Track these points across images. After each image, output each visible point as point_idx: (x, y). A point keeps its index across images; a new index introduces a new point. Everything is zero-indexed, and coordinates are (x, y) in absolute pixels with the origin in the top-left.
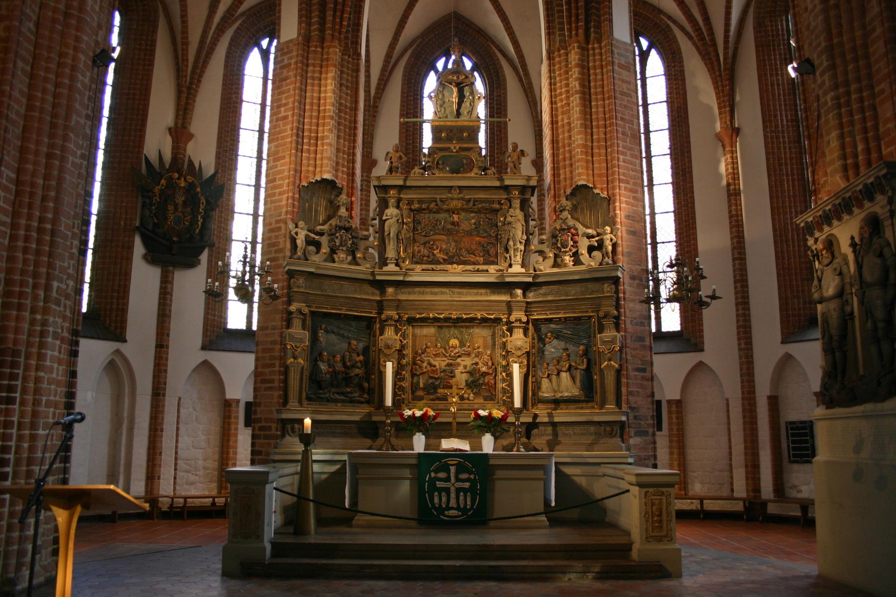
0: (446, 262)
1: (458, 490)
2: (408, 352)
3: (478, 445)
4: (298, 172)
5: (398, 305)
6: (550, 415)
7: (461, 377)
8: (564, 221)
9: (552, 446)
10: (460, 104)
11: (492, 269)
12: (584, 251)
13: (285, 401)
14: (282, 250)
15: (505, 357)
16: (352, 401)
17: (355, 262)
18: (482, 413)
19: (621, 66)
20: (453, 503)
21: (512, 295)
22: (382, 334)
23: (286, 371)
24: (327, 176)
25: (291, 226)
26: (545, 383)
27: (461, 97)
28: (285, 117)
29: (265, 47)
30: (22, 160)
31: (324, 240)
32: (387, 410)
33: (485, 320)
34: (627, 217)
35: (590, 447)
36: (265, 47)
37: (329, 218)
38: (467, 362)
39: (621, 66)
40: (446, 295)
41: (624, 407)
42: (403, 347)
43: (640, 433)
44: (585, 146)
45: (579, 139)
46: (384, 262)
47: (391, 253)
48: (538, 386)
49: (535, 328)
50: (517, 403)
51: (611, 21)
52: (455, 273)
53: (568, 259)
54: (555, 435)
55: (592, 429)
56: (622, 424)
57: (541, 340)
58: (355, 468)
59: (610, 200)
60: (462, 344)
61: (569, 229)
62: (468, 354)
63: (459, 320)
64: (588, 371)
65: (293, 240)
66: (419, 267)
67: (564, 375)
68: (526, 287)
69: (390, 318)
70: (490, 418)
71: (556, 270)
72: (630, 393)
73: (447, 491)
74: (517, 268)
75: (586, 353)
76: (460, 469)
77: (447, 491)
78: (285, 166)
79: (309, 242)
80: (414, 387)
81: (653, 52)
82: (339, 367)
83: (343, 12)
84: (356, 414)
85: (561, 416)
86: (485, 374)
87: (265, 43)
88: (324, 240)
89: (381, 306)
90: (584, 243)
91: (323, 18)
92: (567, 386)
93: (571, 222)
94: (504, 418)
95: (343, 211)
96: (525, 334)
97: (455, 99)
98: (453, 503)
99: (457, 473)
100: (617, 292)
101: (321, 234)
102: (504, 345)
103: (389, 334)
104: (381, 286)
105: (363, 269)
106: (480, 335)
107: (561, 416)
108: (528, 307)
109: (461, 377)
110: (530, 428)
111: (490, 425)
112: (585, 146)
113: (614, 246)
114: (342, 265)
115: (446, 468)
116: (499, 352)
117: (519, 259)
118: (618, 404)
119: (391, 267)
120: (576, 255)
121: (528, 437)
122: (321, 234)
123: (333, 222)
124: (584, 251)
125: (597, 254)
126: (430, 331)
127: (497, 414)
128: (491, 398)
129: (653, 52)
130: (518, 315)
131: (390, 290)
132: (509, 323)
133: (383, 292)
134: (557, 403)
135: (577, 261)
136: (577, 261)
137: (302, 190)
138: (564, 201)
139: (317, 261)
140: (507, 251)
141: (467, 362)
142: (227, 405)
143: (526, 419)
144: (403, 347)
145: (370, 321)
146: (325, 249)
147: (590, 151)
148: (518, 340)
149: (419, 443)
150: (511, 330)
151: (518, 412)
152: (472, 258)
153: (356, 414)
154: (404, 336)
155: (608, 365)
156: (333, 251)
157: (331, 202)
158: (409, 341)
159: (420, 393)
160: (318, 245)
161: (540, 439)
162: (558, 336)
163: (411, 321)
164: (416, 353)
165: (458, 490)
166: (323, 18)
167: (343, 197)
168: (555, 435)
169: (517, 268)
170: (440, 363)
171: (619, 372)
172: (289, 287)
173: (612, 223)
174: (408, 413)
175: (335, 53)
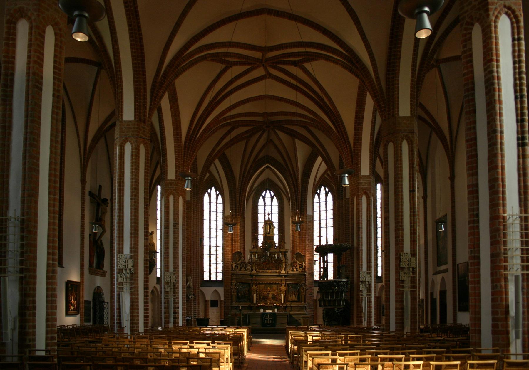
0: (267, 270)
1: (270, 320)
2: (258, 291)
3: (274, 311)
4: (232, 250)
5: (256, 280)
6: (290, 305)
7: (270, 296)
8: (294, 260)
9: (290, 311)
10: (270, 230)
11: (277, 271)
12: (298, 268)
13: (232, 302)
14: (229, 268)
15: (280, 292)
16: (246, 302)
17: (246, 270)
18: (275, 304)
19: (309, 222)
20: (269, 322)
21: (282, 278)
22: (252, 286)
23: (232, 296)
24: (239, 251)
25: (231, 263)
26: (289, 297)
27: (270, 228)
28: (228, 236)
29: (209, 192)
30: (193, 264)
31: (239, 265)
32: (254, 304)
33: (275, 283)
34: (309, 260)
35: (298, 311)
36: (209, 192)
37: (239, 260)
38: (272, 293)
39: (309, 222)
40: (267, 278)
41: (306, 303)
42: (257, 290)
43: (310, 308)
44: (299, 243)
45: (298, 241)
46: (252, 270)
47: (254, 268)
48: (288, 298)
49: (287, 285)
50: (282, 302)
51: (307, 210)
52: (269, 272)
53: (295, 269)
54: (291, 308)
55: (299, 307)
56: (305, 306)
57: (289, 288)
58: (249, 315)
59: (305, 256)
60: (271, 289)
61: (295, 262)
62: (272, 291)
63: (270, 283)
64: (299, 295)
65: (232, 266)
66: (260, 271)
67: (294, 296)
68: (285, 276)
69: (254, 283)
70: (276, 306)
71: (292, 272)
72: (307, 300)
73: (268, 320)
74: (283, 272)
75: (298, 290)
76: (270, 316)
77: (268, 320)
78: (229, 248)
79: (235, 266)
80: (260, 298)
81: (330, 193)
82: (243, 294)
83: (241, 208)
84: (247, 304)
85: (292, 305)
86: (276, 295)
87: (209, 191)
88: (239, 265)
89: (252, 280)
90: (298, 266)
91: (236, 210)
92: (294, 298)
93: (296, 261)
94: (279, 305)
95: (242, 258)
96: (285, 286)
97: (269, 229)
98: (269, 322)
99: (270, 316)
100: (305, 277)
101: (238, 264)
102: (280, 289)
103: (254, 287)
104: (252, 276)
105: (247, 272)
106: (275, 287)
107: (292, 305)
108: (286, 280)
109: (270, 296)
110: (286, 307)
111: (276, 307)
112: (299, 243)
113: (305, 267)
114: (243, 272)
115: (267, 315)
116: (279, 291)
117: (284, 269)
118: (305, 302)
119: (254, 271)
120: (297, 269)
121: (285, 309)
122: (238, 264)
123: (240, 261)
124: (298, 268)
125: (301, 269)
126: (263, 286)
127: (278, 304)
128: (277, 300)
129: (330, 193)
130: (283, 282)
131: (254, 277)
132: (281, 284)
133: (252, 277)
134: (292, 302)
135: (297, 270)
136: (297, 270)
137: (233, 254)
138: (294, 256)
139: (238, 271)
140: (281, 267)
141: (272, 293)
142: (206, 301)
143: (285, 305)
144: (257, 290)
145: (249, 284)
146: (239, 268)
147: (300, 244)
148: (283, 288)
149: (262, 311)
150: (282, 286)
151: (283, 304)
152: (273, 269)
153: (247, 304)
154: (257, 287)
155: (303, 294)
156: (241, 268)
157: (240, 256)
158: (258, 288)
159: (261, 300)
160: (237, 267)
161: (288, 310)
162: (292, 287)
163: (259, 284)
164: (260, 291)
165: (270, 320)
166: (236, 210)
167: (243, 255)
168: (291, 308)
169: (283, 272)
170: (266, 293)
171: (305, 295)
172: (232, 277)
173: (305, 262)
174: (259, 304)
175: (239, 219)
